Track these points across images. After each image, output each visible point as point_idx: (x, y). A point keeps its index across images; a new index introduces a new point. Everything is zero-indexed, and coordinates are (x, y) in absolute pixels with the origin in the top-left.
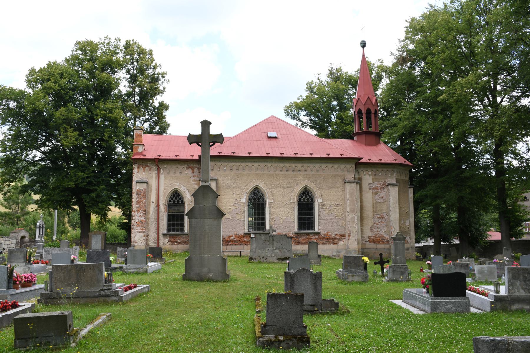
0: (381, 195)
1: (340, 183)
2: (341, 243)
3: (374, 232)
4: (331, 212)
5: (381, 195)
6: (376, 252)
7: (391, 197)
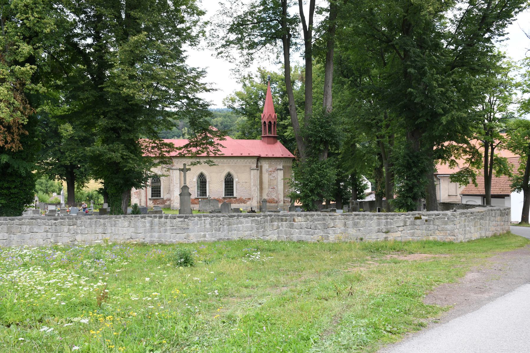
0: (274, 175)
1: (248, 169)
2: (248, 203)
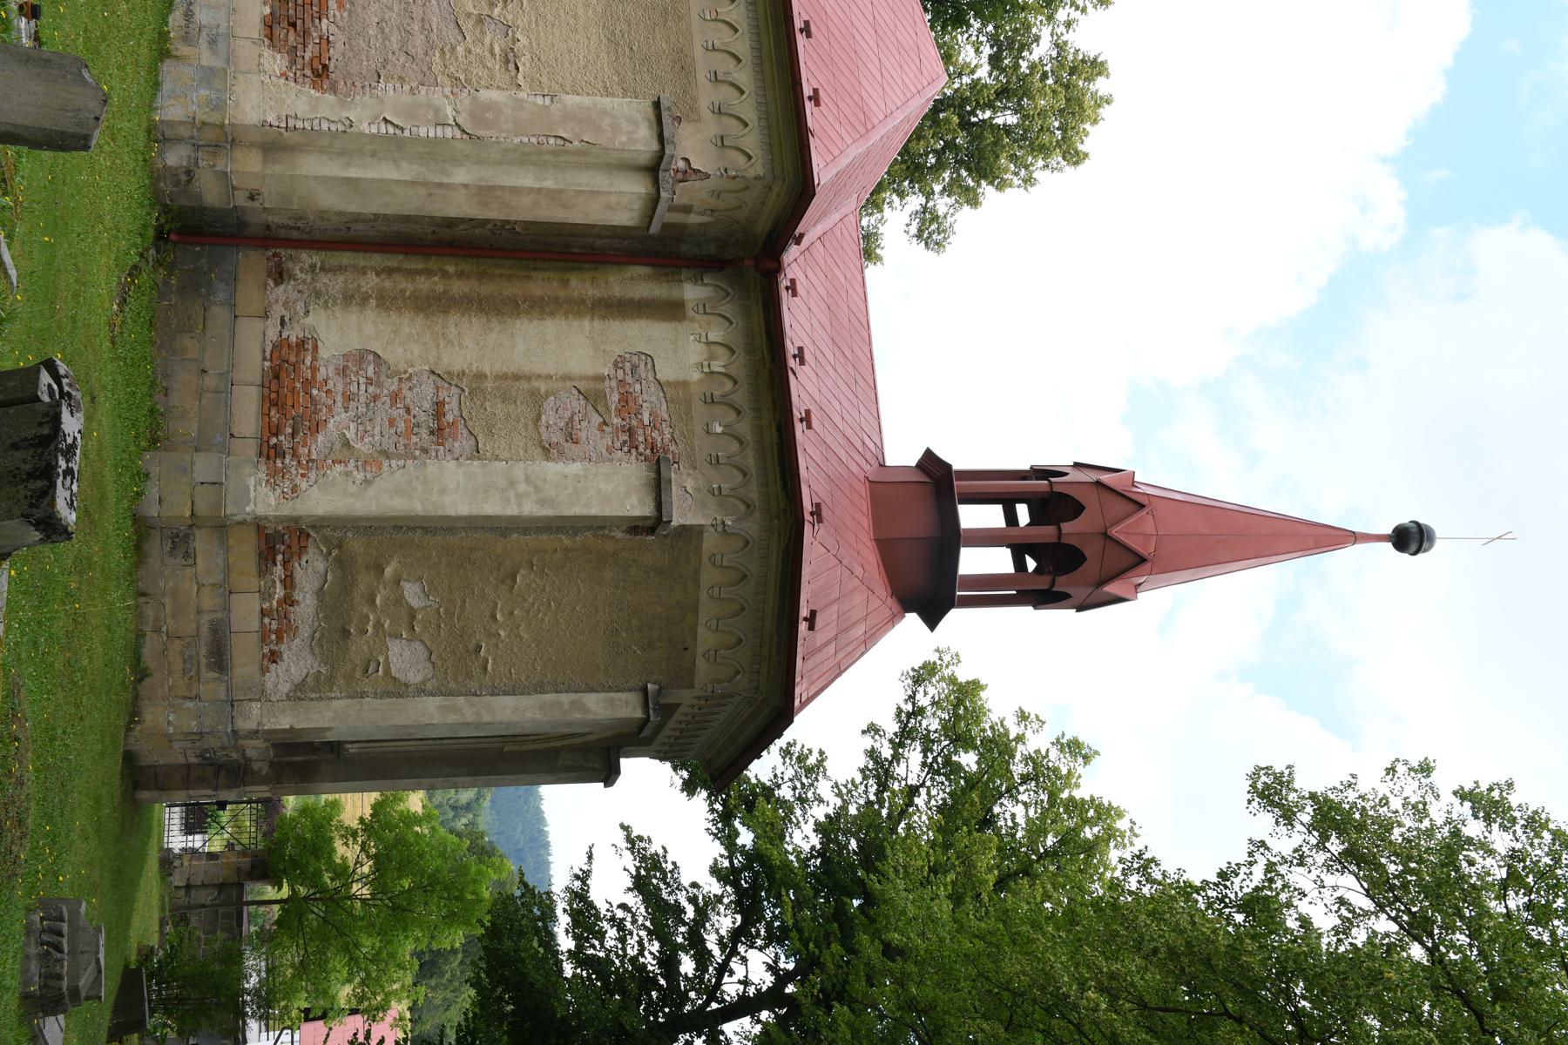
0: (588, 430)
3: (343, 372)
4: (467, 26)
5: (588, 430)
6: (210, 381)
7: (576, 468)
